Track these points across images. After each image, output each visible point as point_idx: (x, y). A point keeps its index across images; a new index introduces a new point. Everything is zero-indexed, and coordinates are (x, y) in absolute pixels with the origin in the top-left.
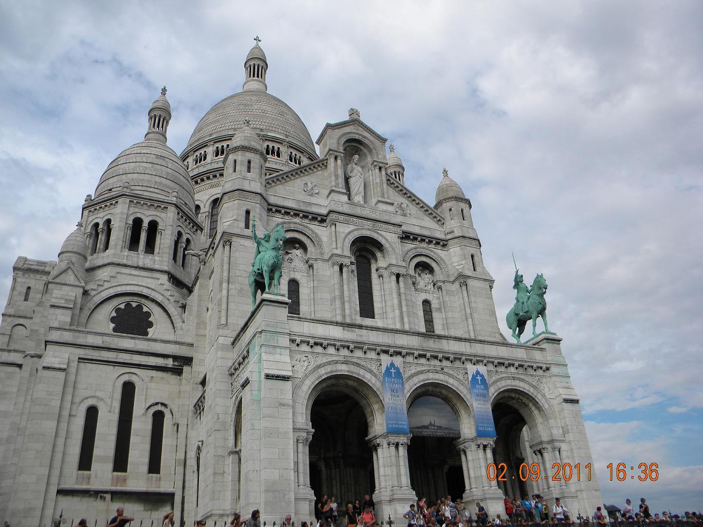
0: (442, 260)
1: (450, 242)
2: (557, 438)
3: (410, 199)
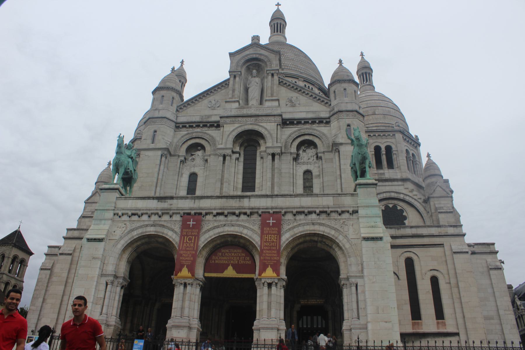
0: (324, 134)
1: (332, 118)
2: (352, 275)
3: (300, 92)
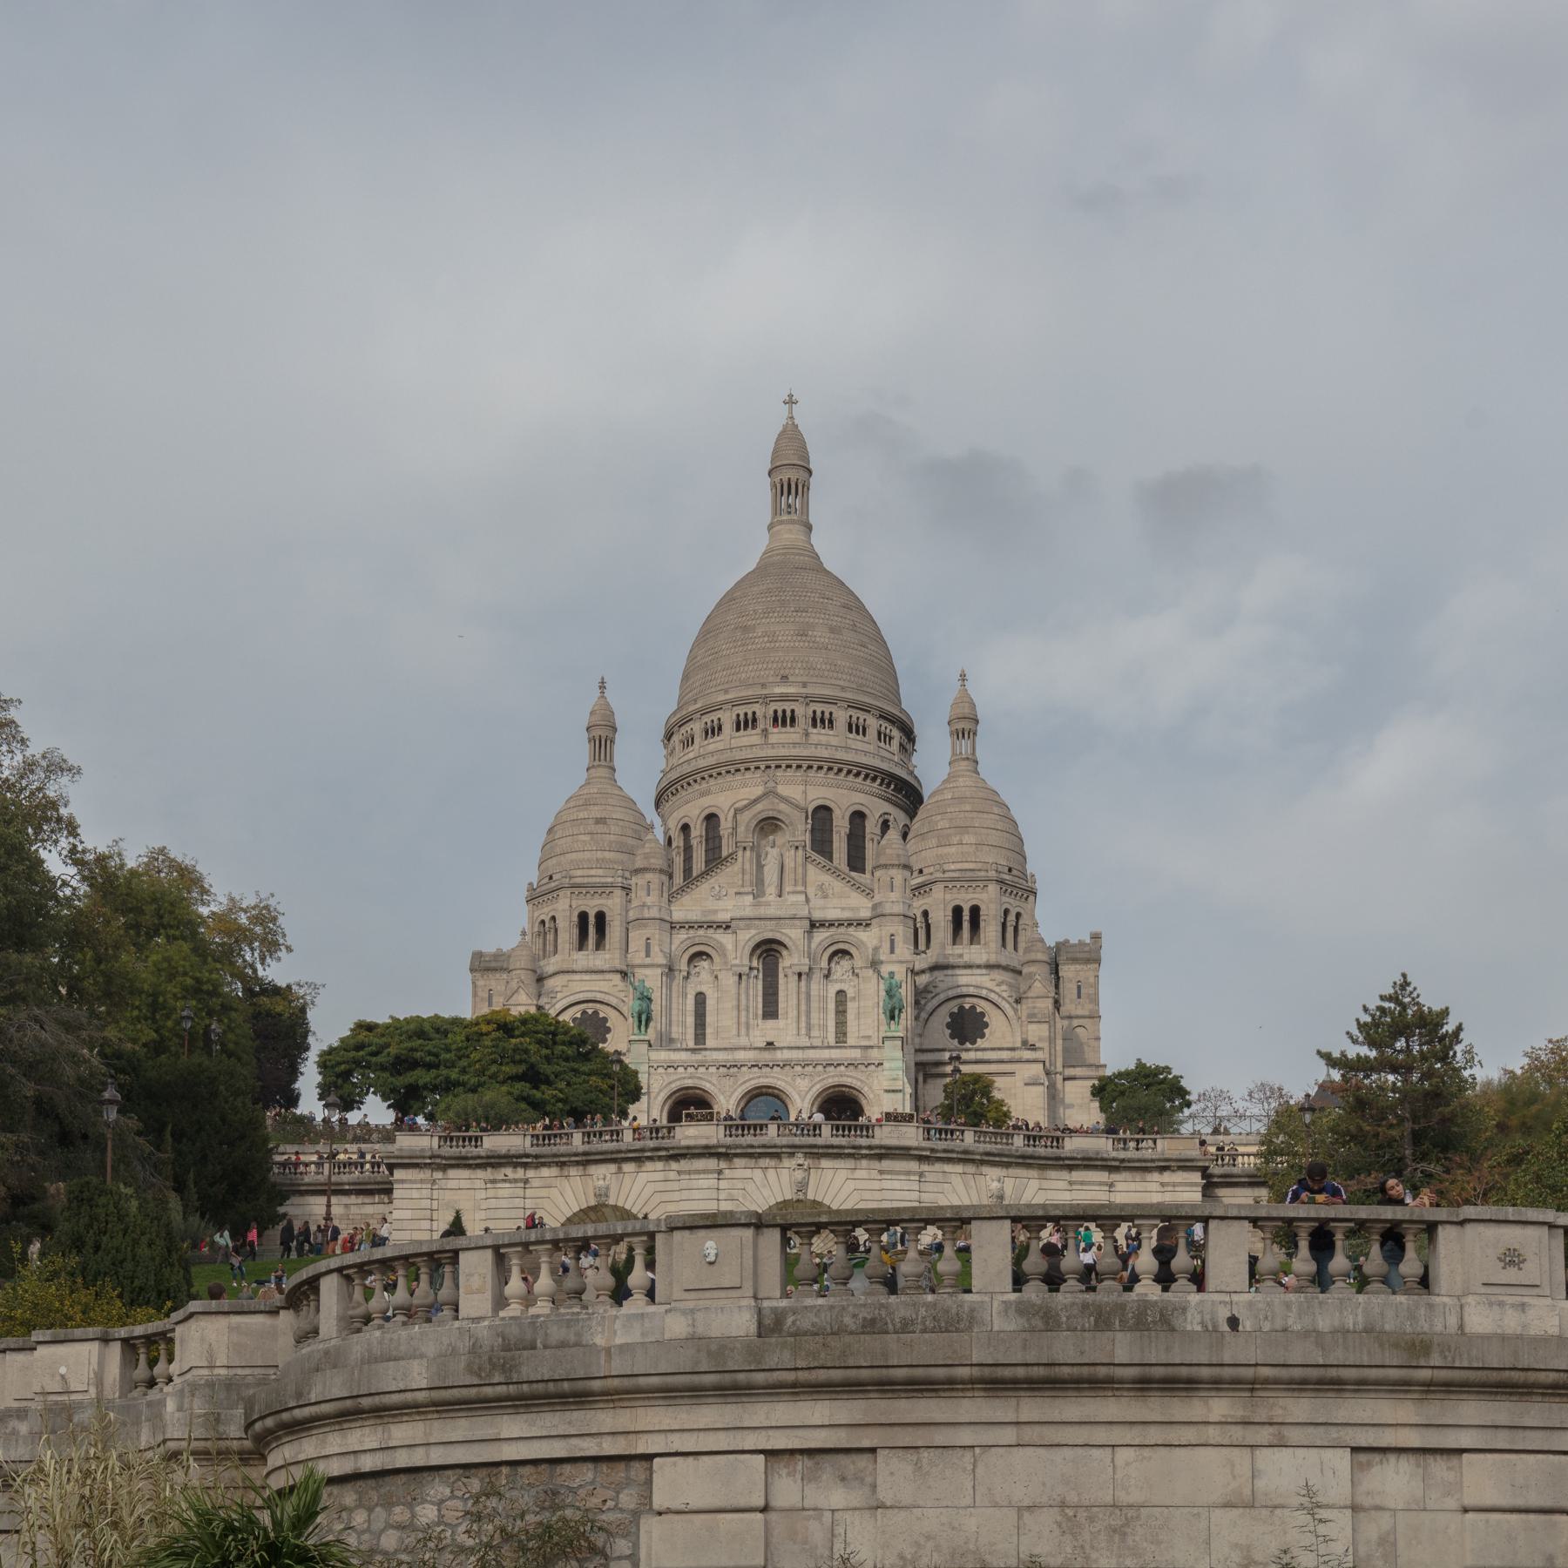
0: (862, 942)
1: (874, 921)
